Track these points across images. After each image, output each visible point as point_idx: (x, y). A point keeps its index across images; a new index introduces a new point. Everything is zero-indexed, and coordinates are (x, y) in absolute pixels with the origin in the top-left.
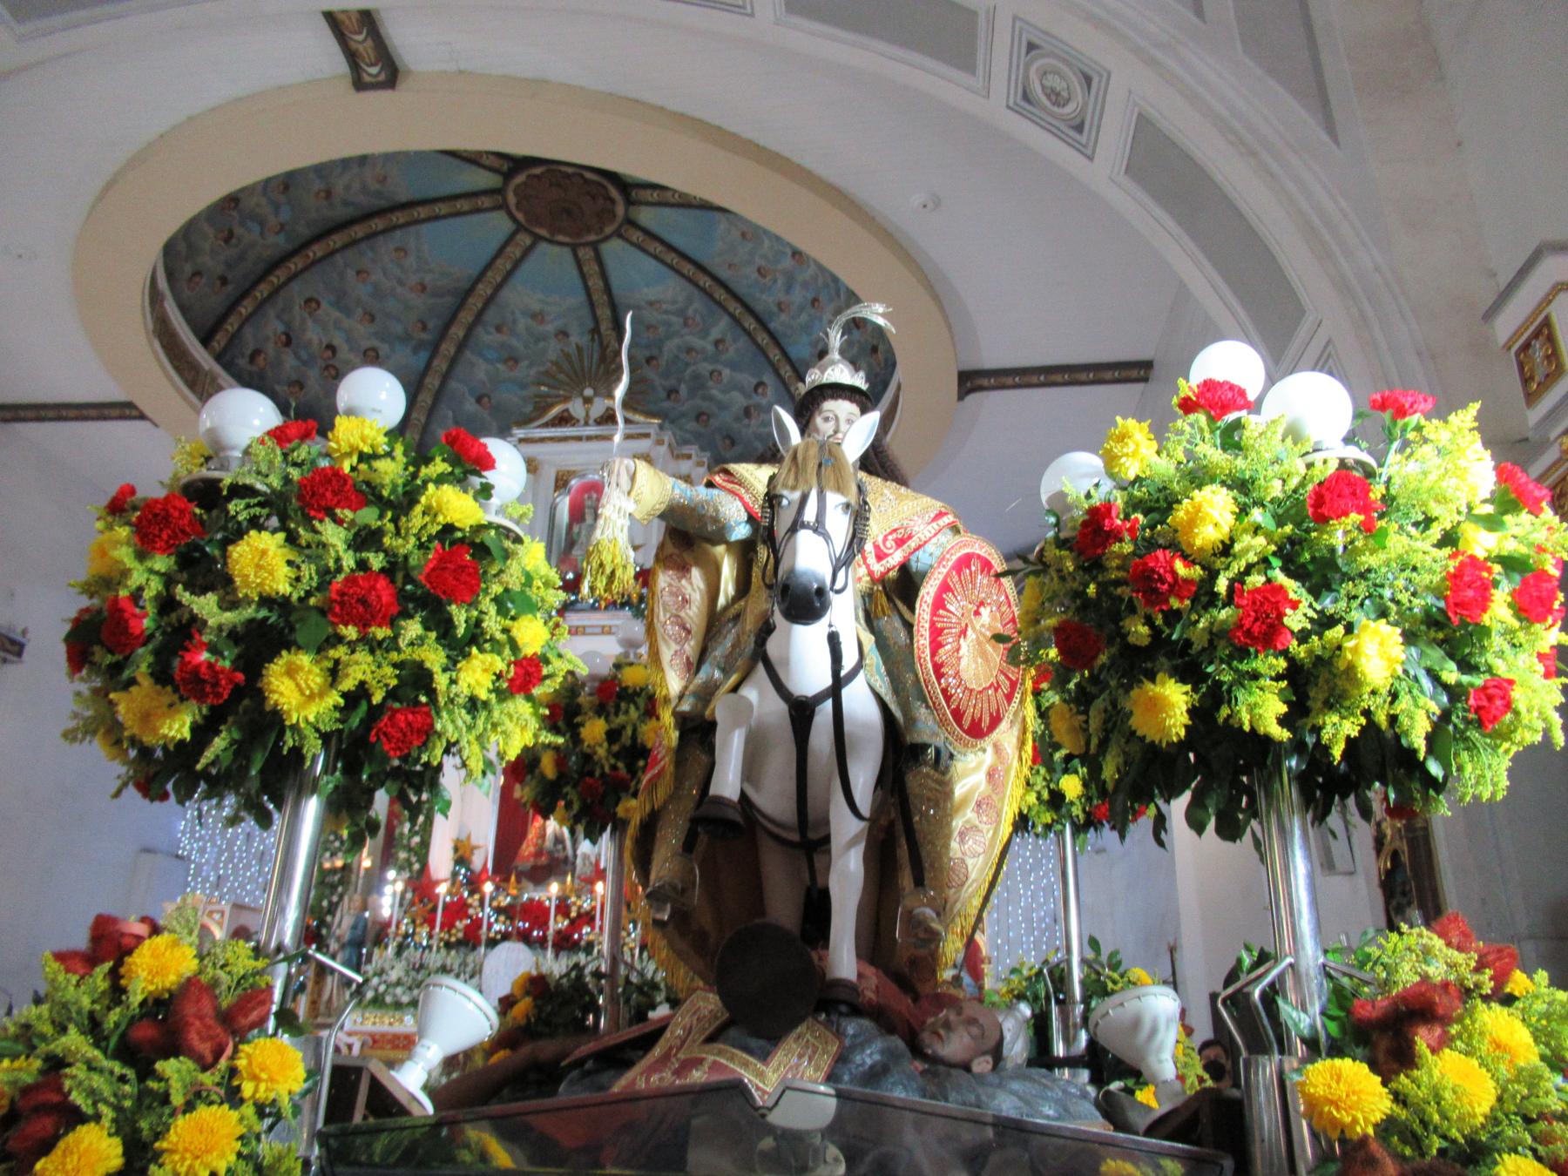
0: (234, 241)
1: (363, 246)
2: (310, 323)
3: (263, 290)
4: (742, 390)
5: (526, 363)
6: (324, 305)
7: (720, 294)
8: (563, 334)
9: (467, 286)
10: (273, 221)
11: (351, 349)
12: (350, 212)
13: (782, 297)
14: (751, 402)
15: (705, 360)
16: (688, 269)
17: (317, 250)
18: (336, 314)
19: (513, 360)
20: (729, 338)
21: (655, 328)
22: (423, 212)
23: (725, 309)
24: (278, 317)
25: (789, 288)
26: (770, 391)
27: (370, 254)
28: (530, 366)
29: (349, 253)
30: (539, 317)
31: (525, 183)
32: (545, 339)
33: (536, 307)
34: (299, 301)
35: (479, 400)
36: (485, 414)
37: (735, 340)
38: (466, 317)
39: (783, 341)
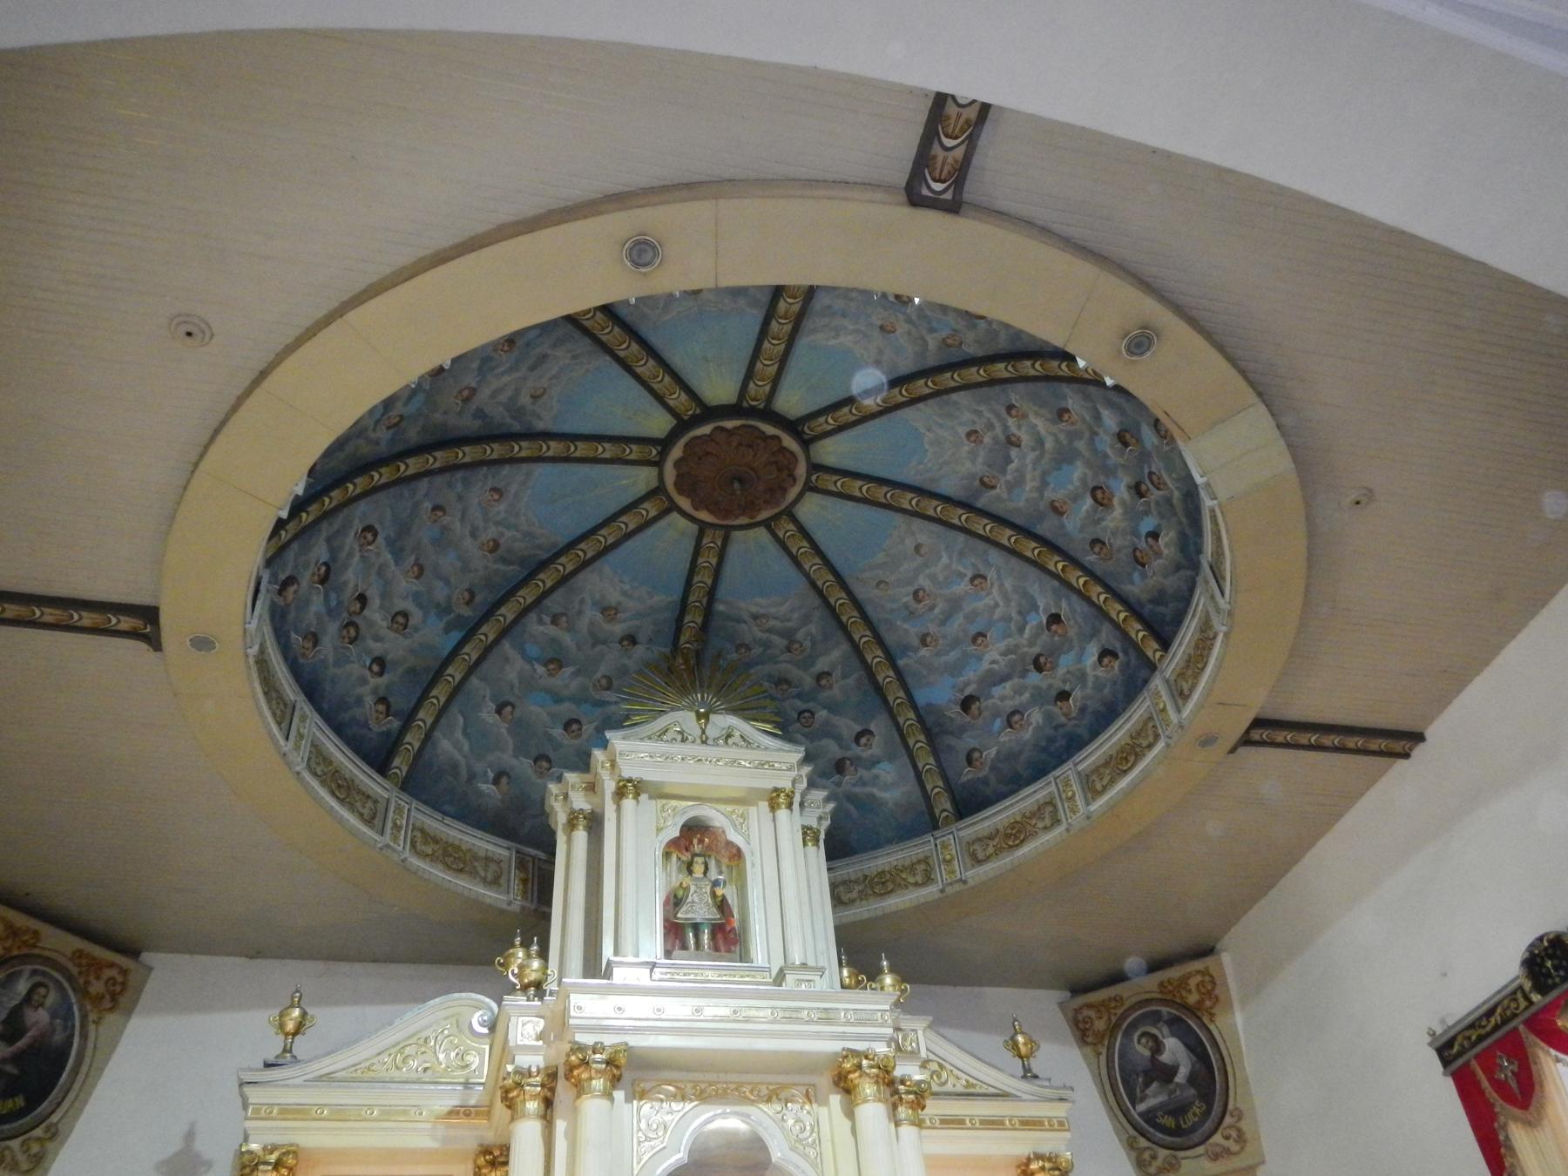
1: (459, 475)
2: (356, 558)
4: (838, 739)
5: (568, 670)
6: (380, 539)
8: (631, 639)
9: (545, 556)
11: (381, 607)
12: (469, 424)
13: (932, 628)
14: (848, 754)
15: (799, 696)
16: (824, 579)
17: (413, 465)
18: (388, 556)
19: (556, 662)
20: (838, 672)
21: (749, 648)
22: (555, 448)
24: (329, 540)
25: (946, 619)
26: (876, 740)
28: (576, 674)
29: (439, 480)
31: (709, 438)
32: (604, 643)
33: (614, 597)
34: (358, 526)
35: (499, 711)
37: (844, 677)
38: (527, 595)
39: (909, 680)
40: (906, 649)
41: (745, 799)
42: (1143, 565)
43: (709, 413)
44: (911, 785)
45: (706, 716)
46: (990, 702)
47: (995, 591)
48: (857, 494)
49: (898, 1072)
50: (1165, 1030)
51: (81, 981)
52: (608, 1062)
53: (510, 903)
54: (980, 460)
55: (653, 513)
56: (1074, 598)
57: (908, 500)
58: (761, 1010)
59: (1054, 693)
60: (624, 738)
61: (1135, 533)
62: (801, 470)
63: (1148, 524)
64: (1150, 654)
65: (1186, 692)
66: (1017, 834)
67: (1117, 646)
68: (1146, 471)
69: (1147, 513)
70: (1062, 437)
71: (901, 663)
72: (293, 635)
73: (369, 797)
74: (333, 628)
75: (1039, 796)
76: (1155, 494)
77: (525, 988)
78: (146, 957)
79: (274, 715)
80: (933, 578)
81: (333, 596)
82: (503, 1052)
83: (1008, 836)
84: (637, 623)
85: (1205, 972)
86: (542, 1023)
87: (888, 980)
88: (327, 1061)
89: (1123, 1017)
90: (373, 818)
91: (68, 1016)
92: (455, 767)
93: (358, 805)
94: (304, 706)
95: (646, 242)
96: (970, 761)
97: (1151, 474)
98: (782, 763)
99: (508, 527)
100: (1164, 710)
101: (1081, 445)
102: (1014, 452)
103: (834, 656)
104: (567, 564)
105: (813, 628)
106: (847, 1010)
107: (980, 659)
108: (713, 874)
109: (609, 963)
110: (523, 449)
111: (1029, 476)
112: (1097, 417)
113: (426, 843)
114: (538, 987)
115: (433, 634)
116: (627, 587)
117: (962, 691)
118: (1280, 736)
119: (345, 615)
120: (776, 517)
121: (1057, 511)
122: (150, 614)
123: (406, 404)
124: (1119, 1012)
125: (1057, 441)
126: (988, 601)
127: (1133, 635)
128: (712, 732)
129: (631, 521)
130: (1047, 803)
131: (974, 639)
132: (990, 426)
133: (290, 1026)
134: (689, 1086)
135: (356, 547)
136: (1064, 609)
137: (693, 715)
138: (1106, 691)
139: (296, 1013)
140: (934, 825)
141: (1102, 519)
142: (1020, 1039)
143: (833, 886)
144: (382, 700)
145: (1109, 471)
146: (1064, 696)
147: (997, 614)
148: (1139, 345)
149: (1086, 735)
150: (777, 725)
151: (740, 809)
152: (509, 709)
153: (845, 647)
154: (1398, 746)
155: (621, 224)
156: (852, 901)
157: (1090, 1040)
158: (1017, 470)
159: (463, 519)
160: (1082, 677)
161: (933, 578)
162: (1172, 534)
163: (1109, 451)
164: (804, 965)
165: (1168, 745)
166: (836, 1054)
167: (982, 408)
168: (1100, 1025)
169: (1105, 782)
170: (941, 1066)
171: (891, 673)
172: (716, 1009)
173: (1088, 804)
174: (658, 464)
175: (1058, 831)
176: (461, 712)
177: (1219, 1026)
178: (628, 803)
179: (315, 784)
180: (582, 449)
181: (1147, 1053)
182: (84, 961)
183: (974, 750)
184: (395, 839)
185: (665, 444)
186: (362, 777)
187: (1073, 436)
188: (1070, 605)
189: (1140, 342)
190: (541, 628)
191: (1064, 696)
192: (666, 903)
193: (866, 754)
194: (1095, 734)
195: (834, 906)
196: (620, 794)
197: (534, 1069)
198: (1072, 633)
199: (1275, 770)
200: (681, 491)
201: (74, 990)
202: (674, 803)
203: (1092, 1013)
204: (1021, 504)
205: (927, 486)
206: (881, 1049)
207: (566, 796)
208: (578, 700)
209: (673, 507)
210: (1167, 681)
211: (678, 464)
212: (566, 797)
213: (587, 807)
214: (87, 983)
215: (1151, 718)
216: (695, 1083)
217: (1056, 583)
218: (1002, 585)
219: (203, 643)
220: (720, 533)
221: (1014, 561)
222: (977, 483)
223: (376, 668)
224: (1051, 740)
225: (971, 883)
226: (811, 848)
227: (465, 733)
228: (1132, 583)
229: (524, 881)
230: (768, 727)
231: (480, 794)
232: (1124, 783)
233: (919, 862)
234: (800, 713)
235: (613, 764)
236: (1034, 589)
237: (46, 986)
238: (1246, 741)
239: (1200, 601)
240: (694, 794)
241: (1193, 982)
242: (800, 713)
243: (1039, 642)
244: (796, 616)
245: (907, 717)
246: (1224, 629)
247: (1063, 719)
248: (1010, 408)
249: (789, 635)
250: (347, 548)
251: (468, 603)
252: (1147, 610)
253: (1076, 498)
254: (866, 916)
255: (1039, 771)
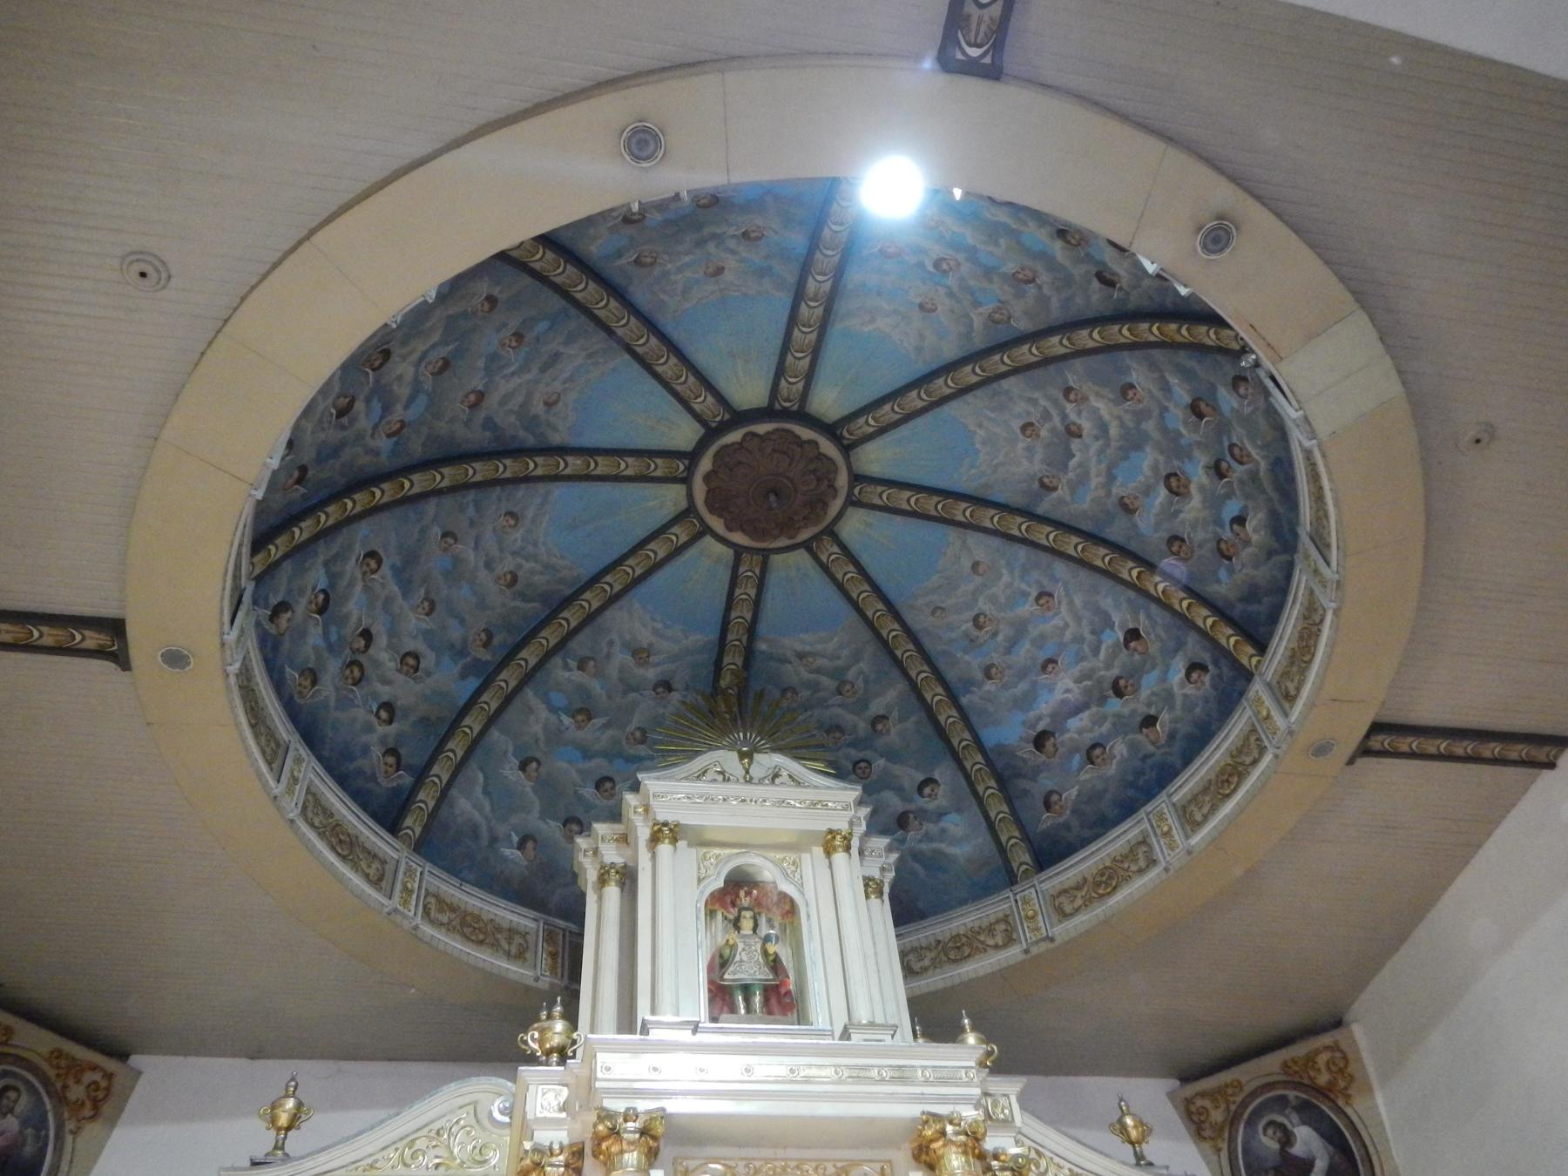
0: (345, 420)
1: (471, 495)
2: (359, 587)
3: (332, 514)
4: (899, 790)
5: (598, 721)
6: (386, 569)
7: (904, 650)
8: (666, 685)
9: (568, 592)
10: (399, 412)
11: (390, 646)
12: (476, 437)
13: (996, 658)
14: (912, 807)
15: (852, 745)
16: (874, 608)
17: (418, 482)
19: (585, 712)
20: (895, 714)
22: (575, 464)
23: (905, 673)
24: (326, 564)
26: (941, 791)
27: (471, 510)
28: (606, 726)
29: (448, 502)
30: (641, 654)
31: (739, 445)
32: (636, 690)
33: (645, 637)
34: (359, 550)
35: (523, 766)
36: (528, 787)
37: (902, 720)
38: (550, 637)
39: (974, 719)
40: (969, 684)
41: (796, 845)
42: (1229, 559)
43: (740, 417)
44: (983, 839)
45: (749, 755)
46: (1067, 736)
47: (1064, 608)
48: (905, 506)
49: (990, 1144)
50: (1295, 1117)
51: (59, 1085)
52: (644, 1132)
53: (537, 979)
54: (1038, 456)
55: (683, 538)
56: (1154, 608)
57: (961, 511)
58: (822, 1070)
59: (1139, 719)
60: (658, 778)
61: (1218, 522)
62: (842, 480)
63: (1232, 508)
64: (1245, 661)
65: (1293, 693)
66: (1108, 880)
67: (1206, 657)
68: (1226, 444)
69: (1229, 496)
70: (1128, 418)
71: (964, 701)
72: (288, 669)
73: (375, 856)
74: (333, 666)
75: (1130, 835)
76: (1239, 471)
77: (548, 1053)
78: (135, 1060)
79: (263, 753)
80: (993, 600)
81: (334, 629)
82: (524, 1128)
83: (1098, 884)
84: (673, 666)
85: (1334, 1048)
86: (565, 1092)
87: (971, 1039)
88: (323, 1157)
89: (1244, 1105)
90: (381, 879)
91: (42, 1124)
92: (475, 832)
93: (363, 864)
94: (298, 748)
95: (646, 130)
96: (1048, 805)
97: (1232, 446)
98: (837, 803)
99: (527, 559)
100: (1268, 717)
101: (1150, 426)
102: (1075, 445)
103: (890, 697)
104: (592, 599)
105: (863, 665)
106: (924, 1068)
107: (1051, 690)
108: (764, 930)
109: (644, 1023)
110: (538, 466)
111: (1093, 472)
112: (1166, 388)
113: (441, 911)
114: (563, 1054)
115: (448, 680)
116: (659, 626)
117: (1033, 726)
118: (1406, 743)
119: (348, 651)
120: (816, 537)
121: (1126, 508)
122: (116, 627)
123: (406, 407)
124: (1239, 1099)
125: (1122, 425)
126: (1057, 621)
127: (1223, 641)
128: (756, 772)
129: (659, 549)
130: (1139, 843)
131: (1044, 667)
132: (1046, 416)
133: (283, 1120)
134: (742, 1164)
135: (359, 576)
136: (1143, 624)
137: (734, 755)
138: (1198, 710)
139: (290, 1104)
140: (1012, 880)
141: (1178, 512)
142: (1129, 1121)
143: (903, 955)
144: (392, 751)
145: (1183, 453)
146: (1149, 721)
147: (1068, 636)
148: (1216, 240)
149: (1177, 761)
150: (830, 764)
151: (791, 856)
152: (534, 765)
153: (902, 685)
154: (1541, 754)
155: (615, 109)
156: (926, 969)
157: (1207, 1133)
158: (1080, 465)
159: (476, 548)
160: (1169, 697)
161: (993, 600)
162: (1261, 515)
163: (1183, 431)
164: (872, 1025)
165: (1276, 756)
166: (914, 1120)
167: (1036, 395)
168: (1217, 1116)
169: (1205, 810)
170: (1037, 1152)
171: (954, 713)
172: (771, 1068)
173: (1187, 837)
174: (686, 480)
175: (1154, 873)
176: (481, 769)
177: (1357, 1108)
178: (664, 849)
179: (311, 835)
180: (603, 466)
181: (1275, 1146)
182: (63, 1063)
183: (1051, 792)
184: (405, 903)
185: (693, 457)
186: (367, 832)
187: (1141, 416)
188: (1149, 616)
189: (1218, 237)
190: (567, 674)
191: (1149, 721)
192: (710, 969)
193: (932, 806)
194: (1187, 760)
195: (905, 977)
196: (655, 839)
197: (556, 1147)
198: (1154, 648)
199: (1399, 782)
200: (712, 510)
201: (48, 1093)
202: (717, 851)
203: (1207, 1103)
204: (1086, 506)
205: (980, 494)
206: (969, 1113)
207: (596, 851)
208: (608, 755)
209: (706, 530)
210: (1269, 685)
211: (707, 478)
212: (597, 849)
213: (619, 860)
214: (65, 1087)
215: (1253, 730)
216: (748, 1160)
217: (1132, 594)
218: (1071, 602)
219: (175, 659)
220: (758, 558)
221: (1083, 574)
222: (1036, 485)
223: (384, 714)
224: (1139, 773)
225: (1059, 940)
226: (874, 901)
227: (486, 792)
228: (1218, 581)
229: (553, 955)
230: (820, 766)
231: (505, 859)
232: (1228, 807)
233: (998, 922)
234: (856, 764)
235: (647, 809)
236: (1107, 603)
237: (16, 1089)
238: (1364, 751)
239: (1301, 581)
240: (733, 840)
241: (1323, 1058)
242: (856, 764)
243: (1117, 663)
244: (845, 652)
245: (974, 761)
246: (1333, 605)
247: (1151, 748)
248: (1068, 391)
249: (838, 674)
250: (348, 576)
251: (486, 645)
252: (1238, 611)
253: (1148, 491)
254: (941, 985)
255: (1128, 809)
